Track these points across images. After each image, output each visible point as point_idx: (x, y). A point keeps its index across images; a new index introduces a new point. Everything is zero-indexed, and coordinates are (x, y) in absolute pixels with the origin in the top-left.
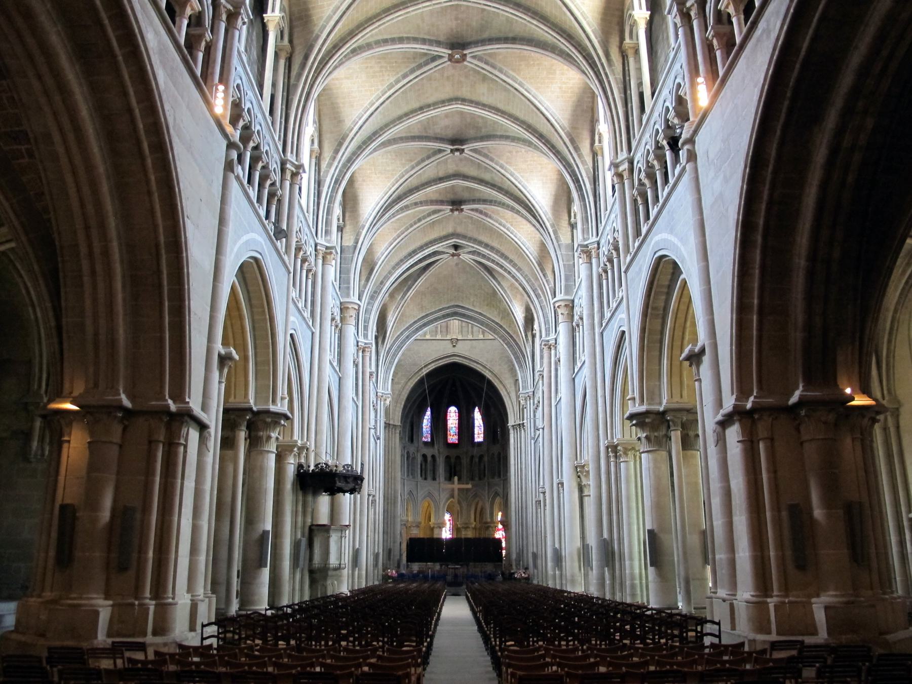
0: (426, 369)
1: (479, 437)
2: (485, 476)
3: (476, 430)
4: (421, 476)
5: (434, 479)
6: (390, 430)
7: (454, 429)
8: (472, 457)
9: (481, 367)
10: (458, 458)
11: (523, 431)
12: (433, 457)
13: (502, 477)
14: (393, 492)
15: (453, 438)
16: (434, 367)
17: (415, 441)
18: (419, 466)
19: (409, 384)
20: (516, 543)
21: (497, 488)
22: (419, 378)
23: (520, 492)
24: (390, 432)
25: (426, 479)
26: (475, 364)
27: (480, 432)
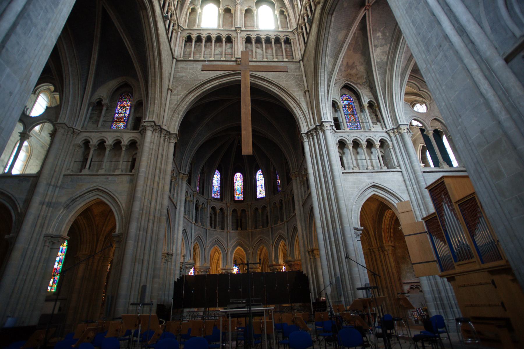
0: (209, 85)
1: (261, 193)
2: (268, 223)
3: (258, 189)
4: (211, 225)
5: (223, 229)
6: (162, 135)
7: (240, 189)
8: (256, 209)
9: (267, 84)
10: (243, 211)
11: (321, 133)
12: (221, 210)
13: (285, 219)
14: (158, 208)
15: (239, 196)
16: (217, 84)
17: (205, 194)
18: (209, 216)
19: (190, 97)
20: (329, 271)
21: (281, 231)
22: (201, 92)
23: (326, 201)
24: (162, 138)
25: (215, 228)
26: (261, 82)
27: (261, 190)
